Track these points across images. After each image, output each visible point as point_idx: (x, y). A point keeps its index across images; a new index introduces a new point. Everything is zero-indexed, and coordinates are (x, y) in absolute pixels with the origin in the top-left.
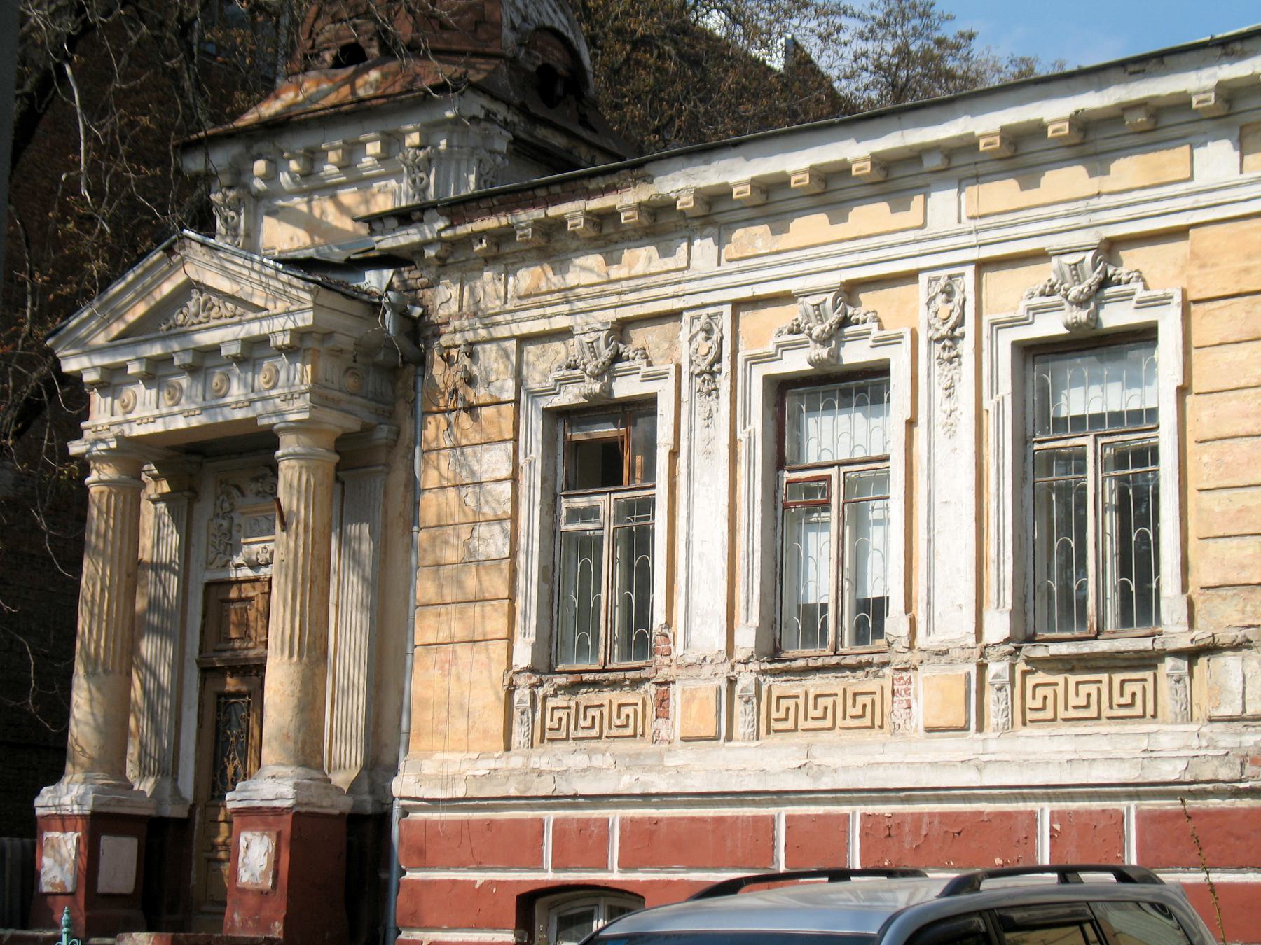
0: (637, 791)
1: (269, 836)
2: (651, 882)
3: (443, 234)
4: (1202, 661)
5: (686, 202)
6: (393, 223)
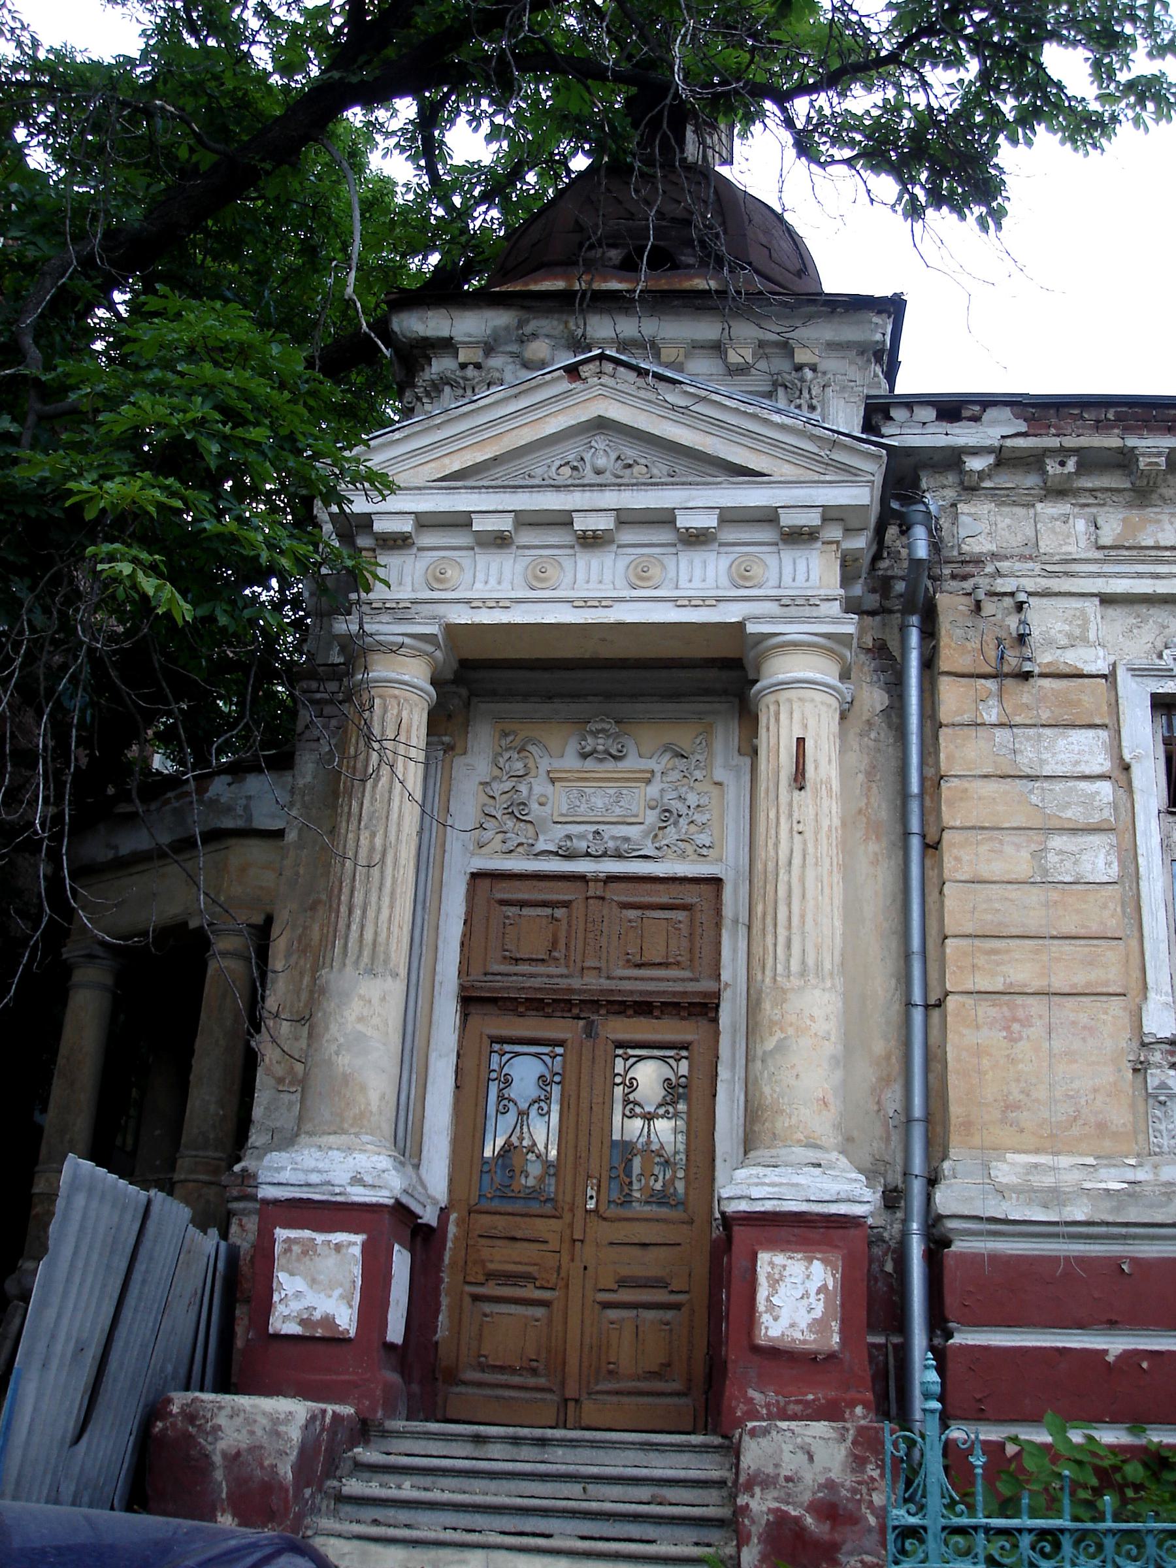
1: (825, 1262)
3: (1009, 443)
6: (929, 414)
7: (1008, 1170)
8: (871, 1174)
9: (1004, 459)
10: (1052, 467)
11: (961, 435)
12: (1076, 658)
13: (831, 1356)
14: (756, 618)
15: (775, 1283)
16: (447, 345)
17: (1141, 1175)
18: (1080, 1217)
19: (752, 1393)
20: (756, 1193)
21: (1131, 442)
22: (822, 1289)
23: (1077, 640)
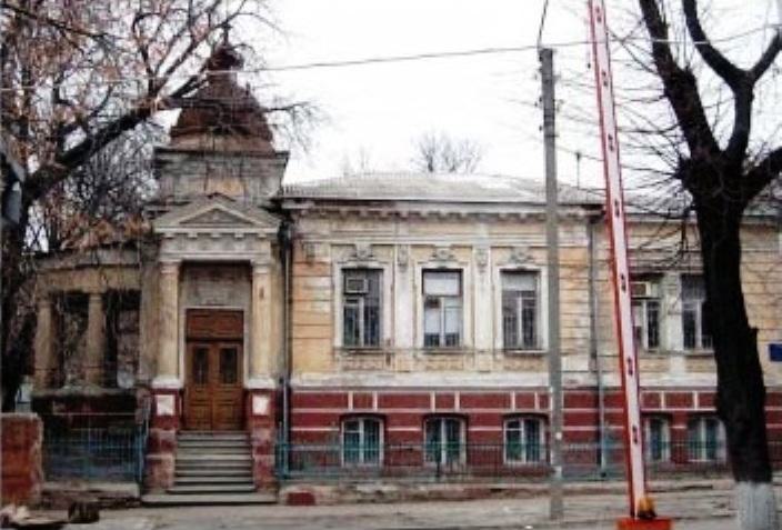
5: (404, 214)
7: (304, 376)
8: (273, 376)
9: (310, 211)
11: (299, 206)
16: (171, 162)
23: (326, 255)
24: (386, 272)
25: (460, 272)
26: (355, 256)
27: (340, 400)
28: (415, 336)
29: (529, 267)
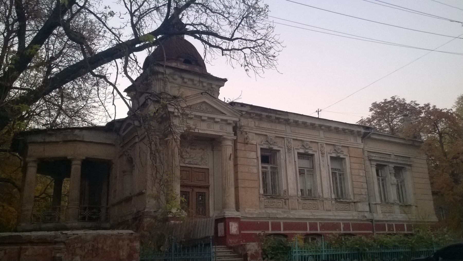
0: (288, 217)
1: (237, 223)
2: (289, 233)
3: (248, 111)
4: (356, 203)
5: (291, 121)
6: (239, 105)
9: (247, 112)
10: (252, 115)
11: (243, 109)
12: (253, 142)
13: (238, 235)
14: (225, 136)
15: (232, 226)
17: (260, 211)
18: (254, 217)
19: (230, 240)
20: (229, 215)
21: (262, 113)
22: (237, 227)
24: (281, 152)
25: (312, 155)
26: (267, 141)
27: (264, 226)
28: (298, 190)
29: (342, 156)
